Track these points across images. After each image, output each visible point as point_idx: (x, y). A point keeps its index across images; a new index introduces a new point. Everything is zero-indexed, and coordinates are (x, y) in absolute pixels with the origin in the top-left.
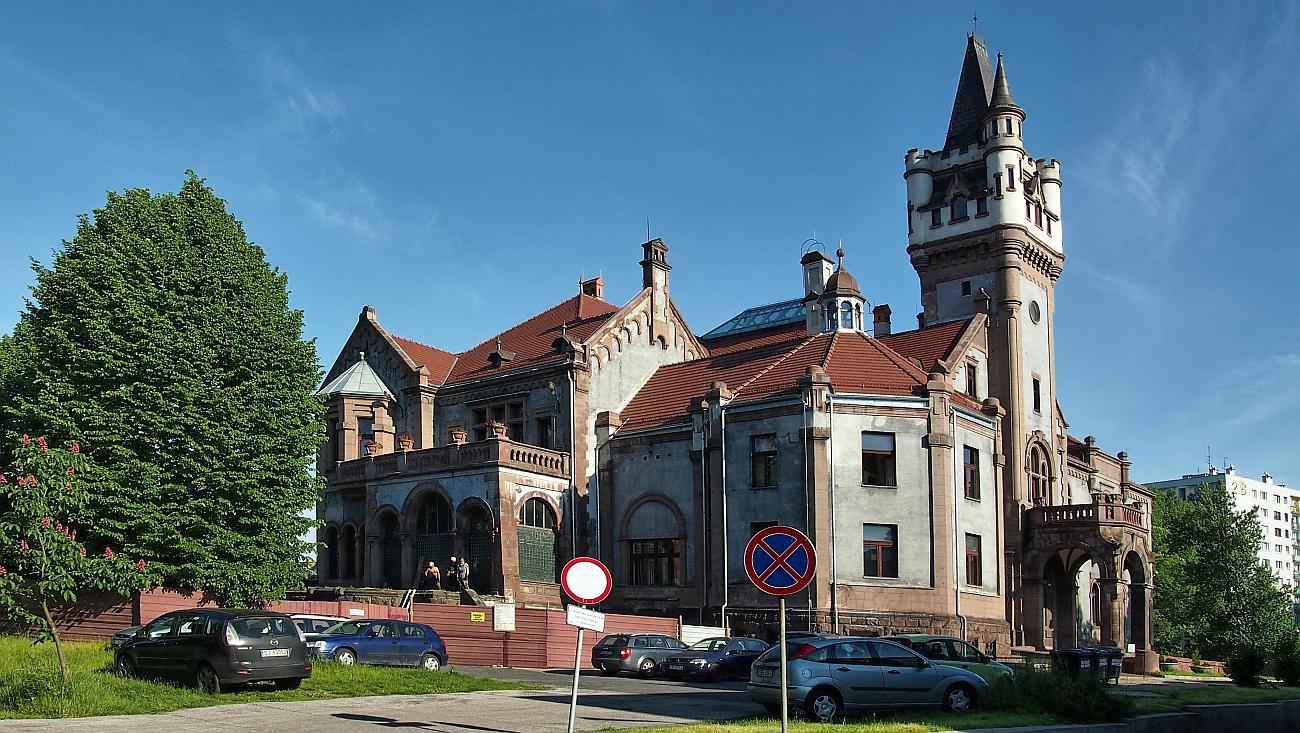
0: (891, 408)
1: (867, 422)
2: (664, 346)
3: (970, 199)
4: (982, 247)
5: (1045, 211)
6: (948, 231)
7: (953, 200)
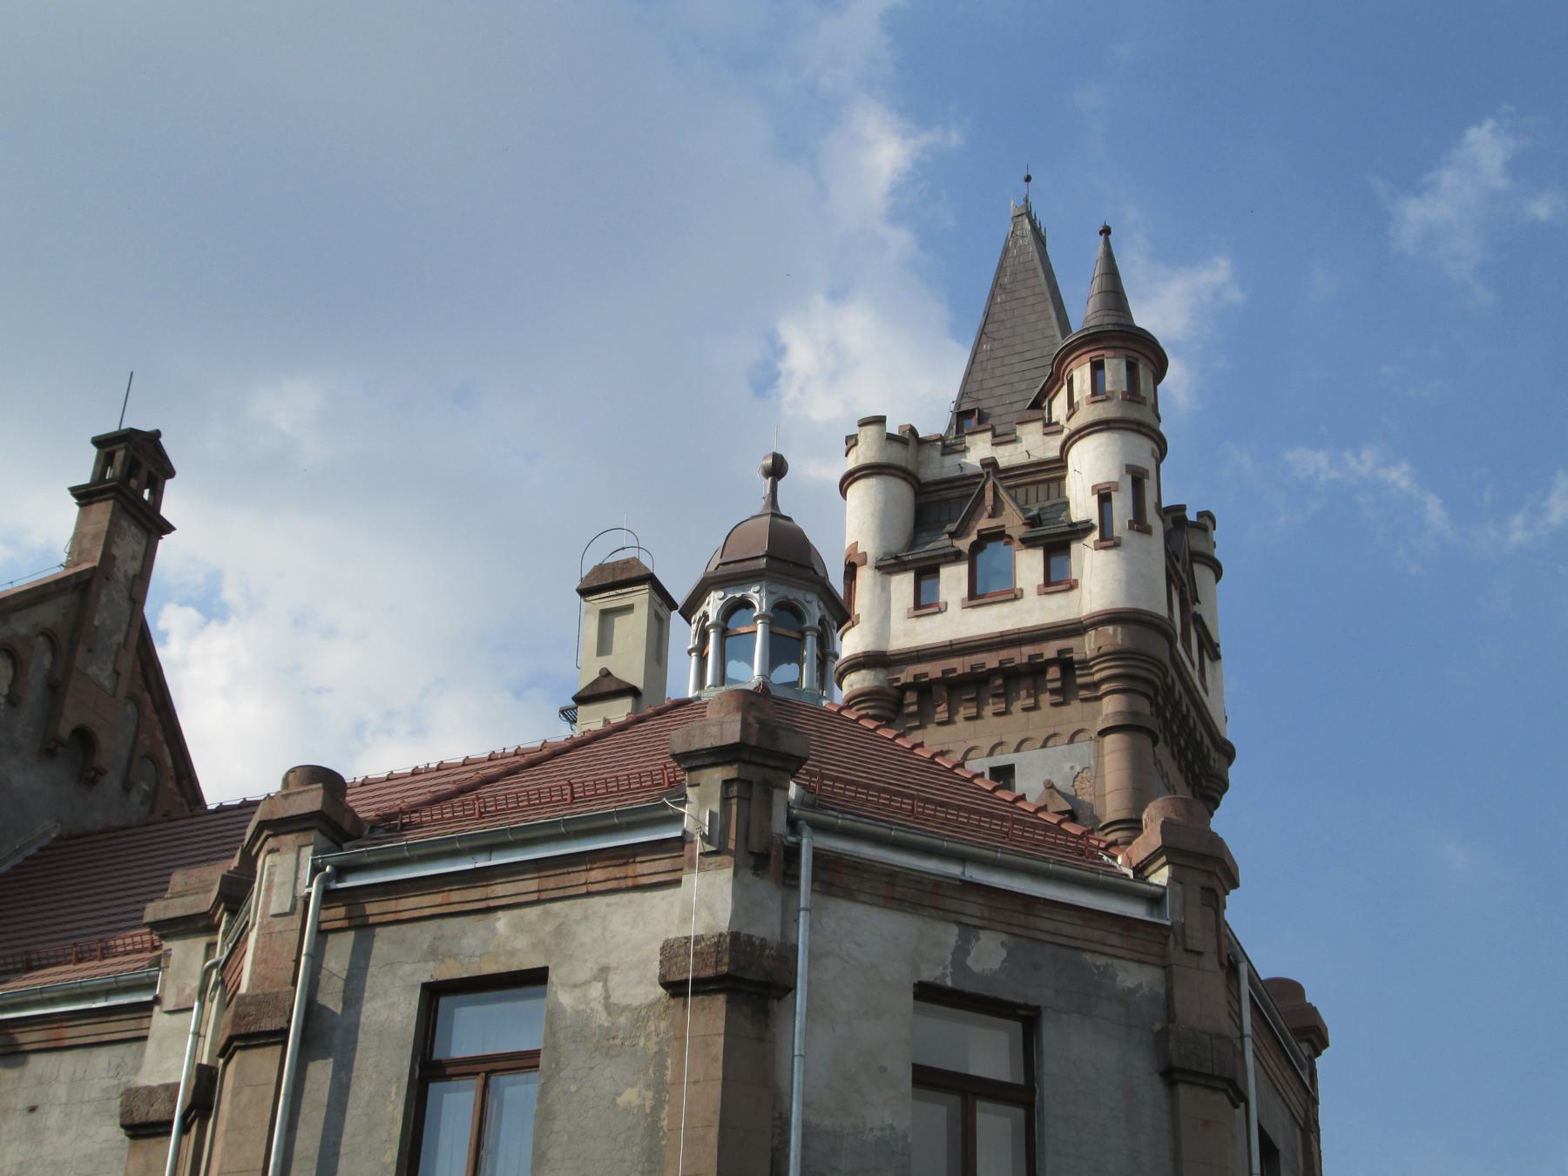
0: (1030, 903)
1: (929, 946)
2: (89, 777)
3: (1028, 543)
4: (1053, 672)
5: (1198, 620)
6: (959, 620)
7: (977, 548)
